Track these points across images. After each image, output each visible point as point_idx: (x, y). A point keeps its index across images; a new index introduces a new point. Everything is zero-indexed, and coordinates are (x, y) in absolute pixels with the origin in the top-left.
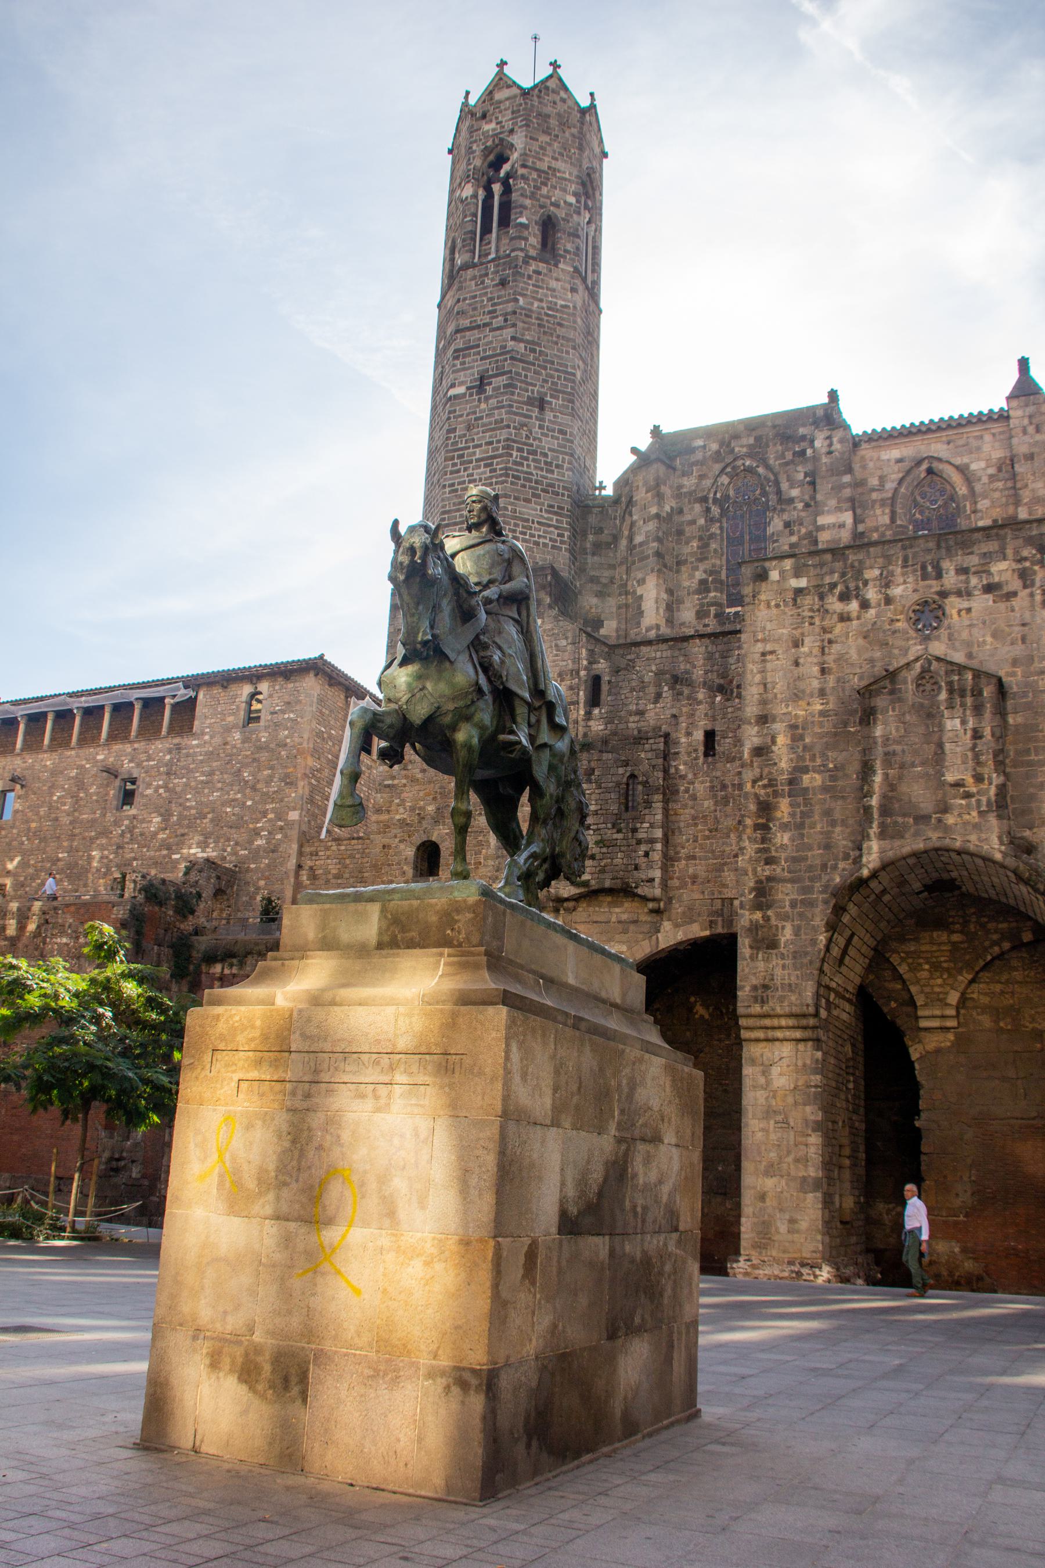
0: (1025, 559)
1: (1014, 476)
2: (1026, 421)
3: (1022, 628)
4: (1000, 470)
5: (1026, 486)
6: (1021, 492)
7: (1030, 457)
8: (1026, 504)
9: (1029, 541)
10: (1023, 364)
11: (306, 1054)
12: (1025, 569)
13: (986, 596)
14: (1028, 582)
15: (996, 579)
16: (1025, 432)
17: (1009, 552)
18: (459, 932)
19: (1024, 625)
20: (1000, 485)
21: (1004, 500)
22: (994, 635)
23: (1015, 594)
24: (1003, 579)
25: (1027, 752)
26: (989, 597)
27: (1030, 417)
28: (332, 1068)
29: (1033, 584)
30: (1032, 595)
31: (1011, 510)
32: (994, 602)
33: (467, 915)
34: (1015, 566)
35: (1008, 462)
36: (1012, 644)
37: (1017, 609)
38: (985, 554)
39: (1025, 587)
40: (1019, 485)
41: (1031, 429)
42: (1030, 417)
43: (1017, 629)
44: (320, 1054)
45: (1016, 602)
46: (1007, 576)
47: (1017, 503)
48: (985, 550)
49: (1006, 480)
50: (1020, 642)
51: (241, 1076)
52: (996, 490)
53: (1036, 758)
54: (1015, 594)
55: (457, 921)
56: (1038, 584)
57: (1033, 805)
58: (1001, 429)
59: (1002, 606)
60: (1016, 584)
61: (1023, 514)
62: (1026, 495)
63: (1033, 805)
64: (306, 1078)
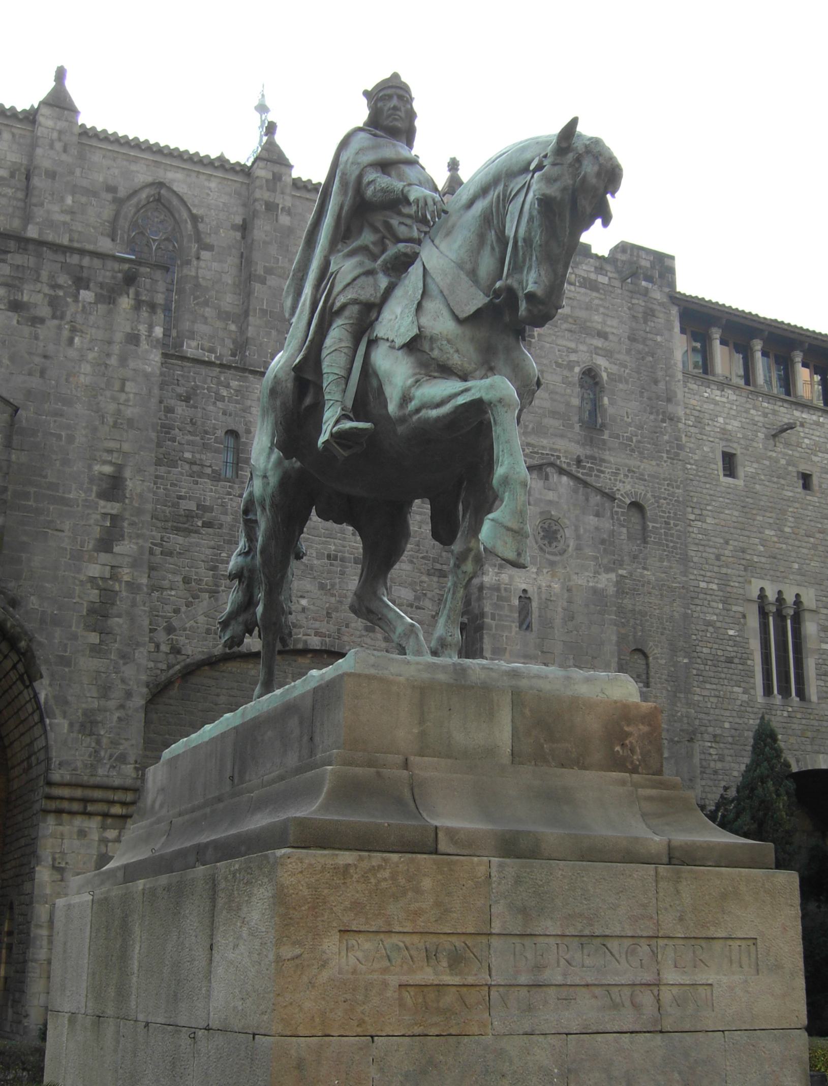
0: (60, 287)
1: (28, 190)
2: (55, 135)
3: (43, 360)
4: (12, 175)
5: (42, 205)
6: (35, 209)
7: (52, 175)
8: (37, 224)
9: (65, 267)
10: (60, 75)
11: (517, 940)
12: (57, 297)
13: (10, 314)
14: (58, 313)
15: (25, 299)
16: (52, 146)
17: (44, 274)
18: (632, 751)
19: (45, 357)
20: (10, 192)
21: (11, 210)
22: (12, 358)
23: (42, 321)
24: (32, 300)
25: (26, 496)
26: (14, 318)
27: (60, 132)
28: (562, 962)
29: (62, 318)
30: (59, 328)
31: (16, 223)
32: (18, 322)
33: (641, 727)
34: (46, 290)
35: (23, 170)
36: (30, 374)
37: (41, 337)
38: (18, 266)
39: (54, 317)
40: (34, 200)
41: (58, 146)
42: (60, 132)
43: (37, 360)
44: (541, 939)
45: (42, 331)
46: (38, 298)
47: (27, 219)
48: (20, 263)
49: (18, 189)
50: (38, 375)
51: (405, 979)
52: (5, 196)
53: (34, 505)
54: (42, 321)
55: (628, 734)
56: (68, 317)
57: (24, 556)
58: (23, 132)
59: (26, 330)
60: (44, 311)
61: (32, 232)
62: (39, 214)
63: (24, 556)
64: (523, 979)
